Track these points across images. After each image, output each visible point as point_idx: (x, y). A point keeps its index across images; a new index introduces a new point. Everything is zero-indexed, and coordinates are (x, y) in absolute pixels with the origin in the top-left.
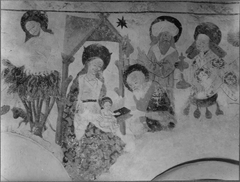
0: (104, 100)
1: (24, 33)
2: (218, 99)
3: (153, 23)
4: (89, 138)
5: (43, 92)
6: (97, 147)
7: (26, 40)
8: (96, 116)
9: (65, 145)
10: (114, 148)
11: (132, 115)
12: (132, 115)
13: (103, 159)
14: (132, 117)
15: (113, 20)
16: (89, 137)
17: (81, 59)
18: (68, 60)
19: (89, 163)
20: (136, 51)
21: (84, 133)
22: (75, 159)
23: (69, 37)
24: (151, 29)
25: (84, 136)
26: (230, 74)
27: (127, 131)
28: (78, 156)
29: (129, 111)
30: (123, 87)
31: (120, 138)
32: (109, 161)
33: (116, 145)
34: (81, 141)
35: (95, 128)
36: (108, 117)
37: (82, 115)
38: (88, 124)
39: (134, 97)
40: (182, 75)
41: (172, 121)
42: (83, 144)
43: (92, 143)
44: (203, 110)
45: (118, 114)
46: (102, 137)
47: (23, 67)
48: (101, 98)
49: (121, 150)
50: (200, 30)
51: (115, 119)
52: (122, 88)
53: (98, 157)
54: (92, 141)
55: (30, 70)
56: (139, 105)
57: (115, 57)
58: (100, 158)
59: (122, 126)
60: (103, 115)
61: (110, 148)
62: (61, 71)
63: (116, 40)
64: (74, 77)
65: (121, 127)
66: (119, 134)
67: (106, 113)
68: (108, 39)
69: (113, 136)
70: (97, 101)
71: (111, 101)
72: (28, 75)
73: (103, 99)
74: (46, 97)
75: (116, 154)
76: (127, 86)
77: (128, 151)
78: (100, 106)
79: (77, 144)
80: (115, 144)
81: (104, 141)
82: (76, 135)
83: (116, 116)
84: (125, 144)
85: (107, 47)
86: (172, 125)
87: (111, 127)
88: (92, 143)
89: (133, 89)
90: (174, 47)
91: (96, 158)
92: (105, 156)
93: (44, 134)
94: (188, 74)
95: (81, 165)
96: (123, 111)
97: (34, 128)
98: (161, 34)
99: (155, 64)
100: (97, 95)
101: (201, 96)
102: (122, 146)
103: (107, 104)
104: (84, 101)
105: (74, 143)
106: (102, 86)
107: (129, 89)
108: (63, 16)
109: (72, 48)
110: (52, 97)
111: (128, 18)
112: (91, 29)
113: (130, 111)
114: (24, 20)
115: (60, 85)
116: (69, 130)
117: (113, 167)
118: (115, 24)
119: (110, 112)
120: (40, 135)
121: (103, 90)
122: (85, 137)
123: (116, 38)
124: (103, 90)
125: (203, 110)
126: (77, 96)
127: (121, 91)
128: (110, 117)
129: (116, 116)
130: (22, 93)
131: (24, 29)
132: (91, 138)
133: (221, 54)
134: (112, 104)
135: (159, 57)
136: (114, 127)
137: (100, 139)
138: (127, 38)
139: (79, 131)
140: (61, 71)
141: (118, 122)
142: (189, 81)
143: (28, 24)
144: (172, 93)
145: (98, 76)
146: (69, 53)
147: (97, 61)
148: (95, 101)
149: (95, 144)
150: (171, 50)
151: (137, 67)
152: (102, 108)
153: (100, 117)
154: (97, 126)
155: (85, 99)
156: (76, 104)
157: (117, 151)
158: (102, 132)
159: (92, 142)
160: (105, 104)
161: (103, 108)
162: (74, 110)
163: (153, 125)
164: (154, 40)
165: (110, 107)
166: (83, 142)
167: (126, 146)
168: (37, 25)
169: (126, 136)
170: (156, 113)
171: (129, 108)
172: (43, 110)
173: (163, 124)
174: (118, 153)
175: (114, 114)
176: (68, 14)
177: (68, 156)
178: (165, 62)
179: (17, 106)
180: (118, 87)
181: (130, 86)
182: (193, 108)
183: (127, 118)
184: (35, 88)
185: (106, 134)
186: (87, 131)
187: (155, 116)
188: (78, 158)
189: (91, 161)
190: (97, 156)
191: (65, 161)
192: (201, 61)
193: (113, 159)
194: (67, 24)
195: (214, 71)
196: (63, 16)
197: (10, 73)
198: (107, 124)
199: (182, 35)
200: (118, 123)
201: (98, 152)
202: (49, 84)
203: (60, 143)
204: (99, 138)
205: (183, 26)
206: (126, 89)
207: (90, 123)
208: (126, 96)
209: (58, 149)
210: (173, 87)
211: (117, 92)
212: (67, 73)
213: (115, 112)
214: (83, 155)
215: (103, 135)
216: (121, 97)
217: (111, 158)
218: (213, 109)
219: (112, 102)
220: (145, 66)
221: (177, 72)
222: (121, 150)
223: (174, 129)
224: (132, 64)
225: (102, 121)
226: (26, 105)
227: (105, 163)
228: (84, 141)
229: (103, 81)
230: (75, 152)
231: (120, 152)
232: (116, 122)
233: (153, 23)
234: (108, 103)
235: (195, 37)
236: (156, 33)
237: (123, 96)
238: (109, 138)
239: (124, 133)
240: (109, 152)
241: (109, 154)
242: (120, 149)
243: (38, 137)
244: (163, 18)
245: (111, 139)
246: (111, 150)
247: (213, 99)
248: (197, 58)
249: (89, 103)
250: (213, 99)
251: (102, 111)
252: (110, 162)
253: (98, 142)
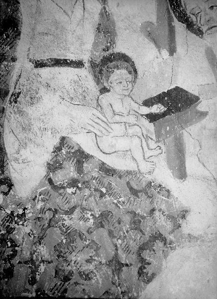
0: (111, 64)
4: (62, 191)
6: (92, 221)
8: (85, 115)
10: (150, 223)
11: (203, 114)
12: (203, 114)
14: (205, 121)
16: (64, 188)
19: (67, 279)
21: (43, 172)
22: (12, 266)
25: (41, 185)
27: (191, 165)
28: (26, 254)
30: (170, 20)
31: (168, 191)
32: (134, 271)
33: (157, 213)
34: (34, 200)
35: (81, 157)
36: (124, 119)
37: (33, 112)
38: (56, 141)
42: (42, 211)
43: (74, 208)
45: (157, 109)
46: (109, 187)
48: (99, 55)
49: (173, 231)
51: (151, 127)
52: (166, 23)
53: (97, 255)
54: (74, 200)
58: (104, 261)
59: (172, 148)
60: (111, 114)
65: (168, 152)
66: (164, 175)
67: (118, 107)
69: (144, 184)
70: (86, 65)
71: (133, 65)
73: (107, 60)
75: (159, 245)
76: (184, 18)
77: (196, 233)
78: (98, 84)
79: (21, 212)
80: (153, 210)
81: (115, 201)
82: (14, 181)
83: (152, 118)
84: (186, 211)
87: (138, 155)
88: (74, 208)
89: (204, 29)
91: (88, 261)
92: (120, 252)
95: (35, 286)
103: (120, 74)
104: (40, 65)
105: (7, 207)
106: (101, 14)
107: (190, 26)
113: (197, 99)
119: (132, 103)
122: (48, 187)
126: (12, 45)
127: (165, 32)
128: (132, 119)
129: (152, 118)
132: (70, 191)
134: (136, 77)
136: (148, 153)
137: (102, 195)
139: (22, 165)
141: (158, 134)
148: (79, 64)
149: (83, 209)
152: (104, 90)
153: (97, 120)
154: (88, 147)
155: (44, 57)
156: (8, 72)
157: (161, 235)
158: (108, 171)
159: (72, 204)
160: (112, 76)
161: (108, 91)
165: (130, 86)
166: (39, 206)
167: (188, 218)
169: (189, 182)
174: (164, 240)
175: (146, 110)
180: (153, 19)
181: (194, 18)
183: (188, 122)
185: (120, 177)
186: (53, 167)
188: (26, 263)
189: (71, 273)
190: (92, 253)
193: (149, 264)
198: (122, 144)
200: (158, 141)
201: (95, 238)
204: (96, 190)
206: (179, 27)
207: (63, 139)
208: (180, 49)
211: (152, 36)
213: (148, 103)
215: (114, 181)
216: (165, 53)
217: (142, 260)
219: (135, 71)
222: (173, 231)
225: (104, 131)
227: (123, 276)
228: (43, 200)
230: (12, 241)
231: (171, 237)
232: (154, 137)
234: (124, 71)
237: (172, 51)
238: (131, 189)
239: (182, 174)
241: (134, 246)
242: (169, 226)
245: (140, 194)
246: (141, 231)
249: (57, 69)
251: (105, 99)
252: (141, 273)
253: (94, 204)
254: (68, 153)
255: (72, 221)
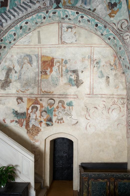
1: (17, 103)
2: (63, 119)
3: (48, 100)
5: (22, 117)
7: (18, 104)
9: (27, 129)
13: (36, 133)
15: (39, 99)
17: (31, 109)
18: (28, 109)
20: (44, 107)
23: (28, 103)
24: (48, 102)
26: (66, 113)
29: (42, 121)
35: (34, 125)
37: (31, 122)
39: (43, 118)
40: (55, 113)
41: (52, 124)
44: (60, 122)
45: (40, 122)
47: (17, 111)
50: (60, 102)
55: (19, 111)
56: (45, 120)
57: (39, 109)
61: (38, 130)
62: (26, 112)
63: (39, 104)
64: (29, 113)
66: (40, 127)
68: (37, 104)
72: (18, 112)
74: (23, 118)
85: (37, 106)
86: (52, 125)
90: (53, 106)
93: (23, 127)
94: (56, 113)
96: (41, 122)
97: (20, 125)
98: (50, 103)
99: (48, 110)
100: (34, 117)
101: (59, 118)
102: (40, 130)
108: (26, 98)
109: (29, 106)
110: (24, 118)
111: (42, 99)
112: (33, 102)
114: (17, 99)
115: (26, 115)
116: (28, 126)
117: (38, 134)
118: (39, 100)
120: (22, 127)
121: (36, 116)
123: (39, 104)
124: (36, 116)
125: (60, 122)
130: (17, 117)
131: (17, 102)
133: (64, 108)
135: (50, 109)
138: (42, 104)
140: (26, 112)
142: (56, 115)
143: (18, 100)
144: (52, 117)
145: (35, 113)
146: (28, 107)
147: (35, 109)
150: (52, 107)
151: (45, 111)
152: (36, 121)
162: (29, 121)
163: (48, 125)
164: (49, 104)
168: (20, 100)
170: (49, 122)
171: (42, 121)
172: (22, 121)
173: (50, 125)
176: (28, 98)
177: (28, 132)
178: (51, 110)
179: (16, 120)
182: (57, 121)
184: (20, 116)
186: (32, 126)
187: (48, 123)
191: (27, 133)
192: (60, 110)
194: (28, 101)
195: (62, 112)
196: (26, 98)
197: (14, 112)
199: (55, 103)
202: (24, 115)
203: (26, 129)
205: (56, 101)
206: (41, 116)
209: (26, 130)
210: (53, 116)
212: (28, 112)
214: (32, 132)
218: (62, 121)
220: (46, 111)
221: (54, 112)
223: (53, 126)
224: (43, 110)
226: (18, 120)
229: (36, 114)
233: (48, 100)
235: (58, 104)
236: (49, 103)
237: (41, 118)
239: (41, 127)
240: (38, 131)
243: (21, 127)
244: (51, 99)
247: (62, 119)
248: (59, 109)
250: (62, 119)
251: (36, 121)
254: (33, 125)
255: (33, 130)
